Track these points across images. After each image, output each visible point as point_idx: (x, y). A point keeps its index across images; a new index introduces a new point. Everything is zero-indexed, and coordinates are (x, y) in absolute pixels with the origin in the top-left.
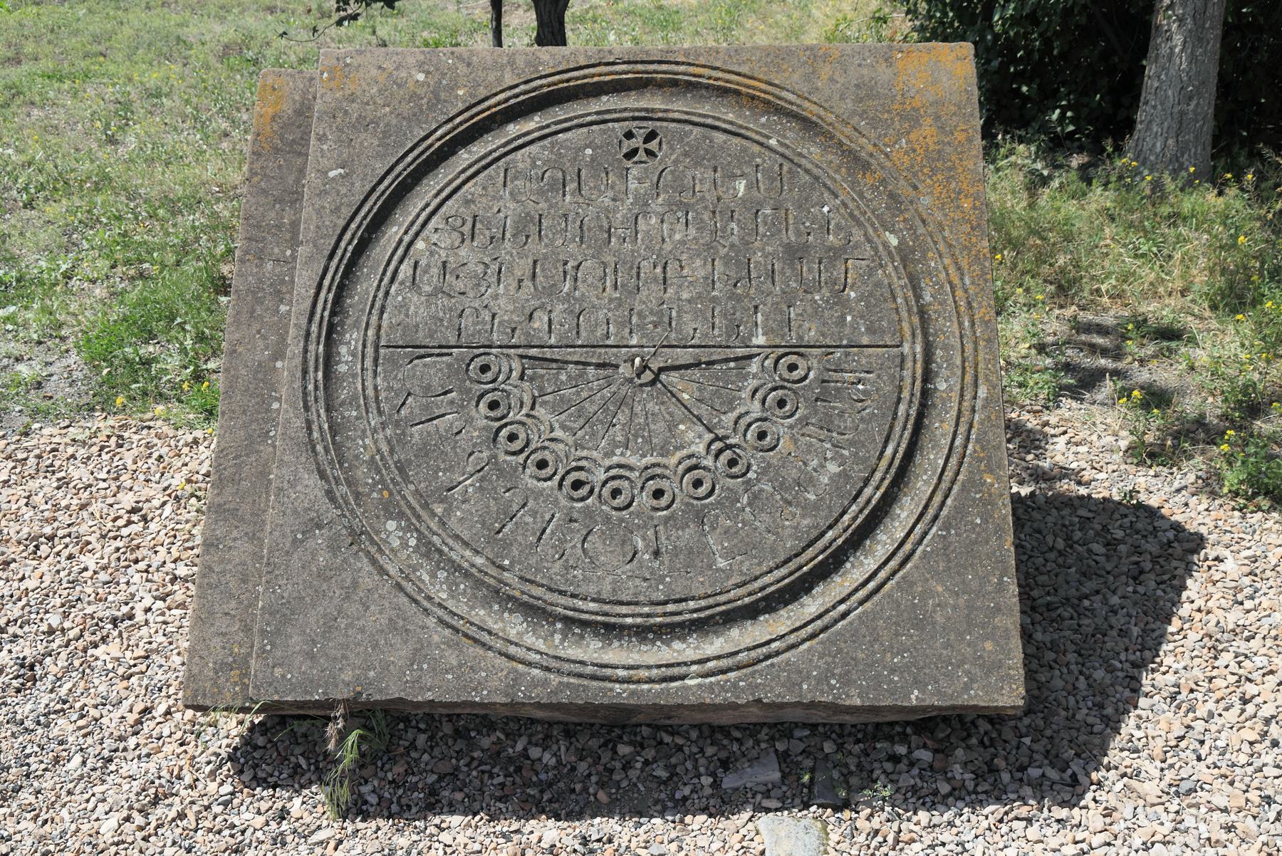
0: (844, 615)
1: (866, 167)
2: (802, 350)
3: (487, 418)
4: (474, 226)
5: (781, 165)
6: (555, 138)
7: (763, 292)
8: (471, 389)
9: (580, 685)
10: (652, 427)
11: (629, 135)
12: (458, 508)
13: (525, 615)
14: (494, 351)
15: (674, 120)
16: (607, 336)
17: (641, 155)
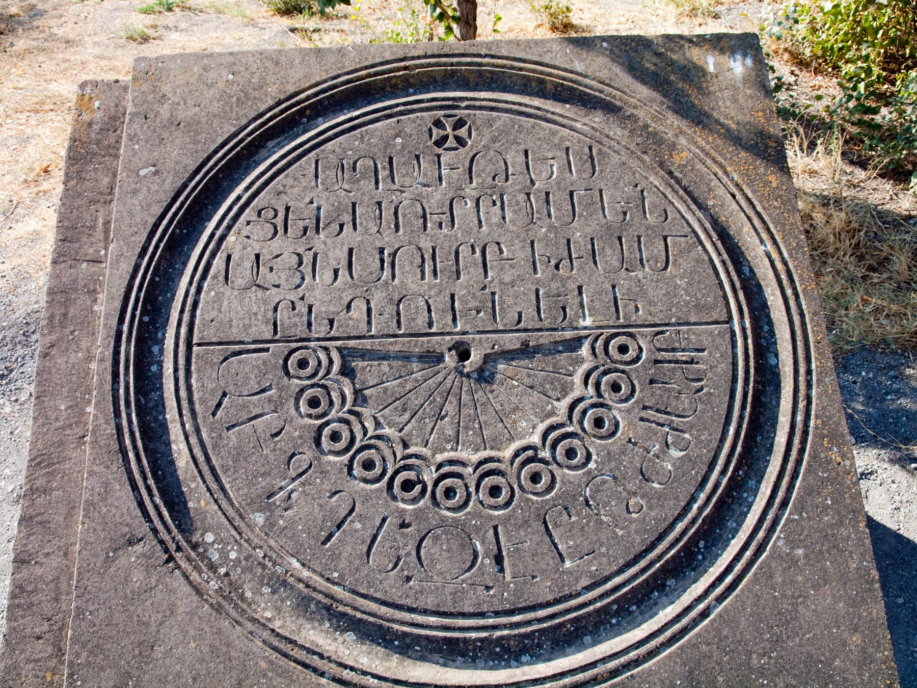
0: (704, 614)
5: (590, 148)
10: (482, 418)
11: (438, 123)
14: (312, 344)
15: (481, 108)
16: (430, 325)
17: (452, 142)
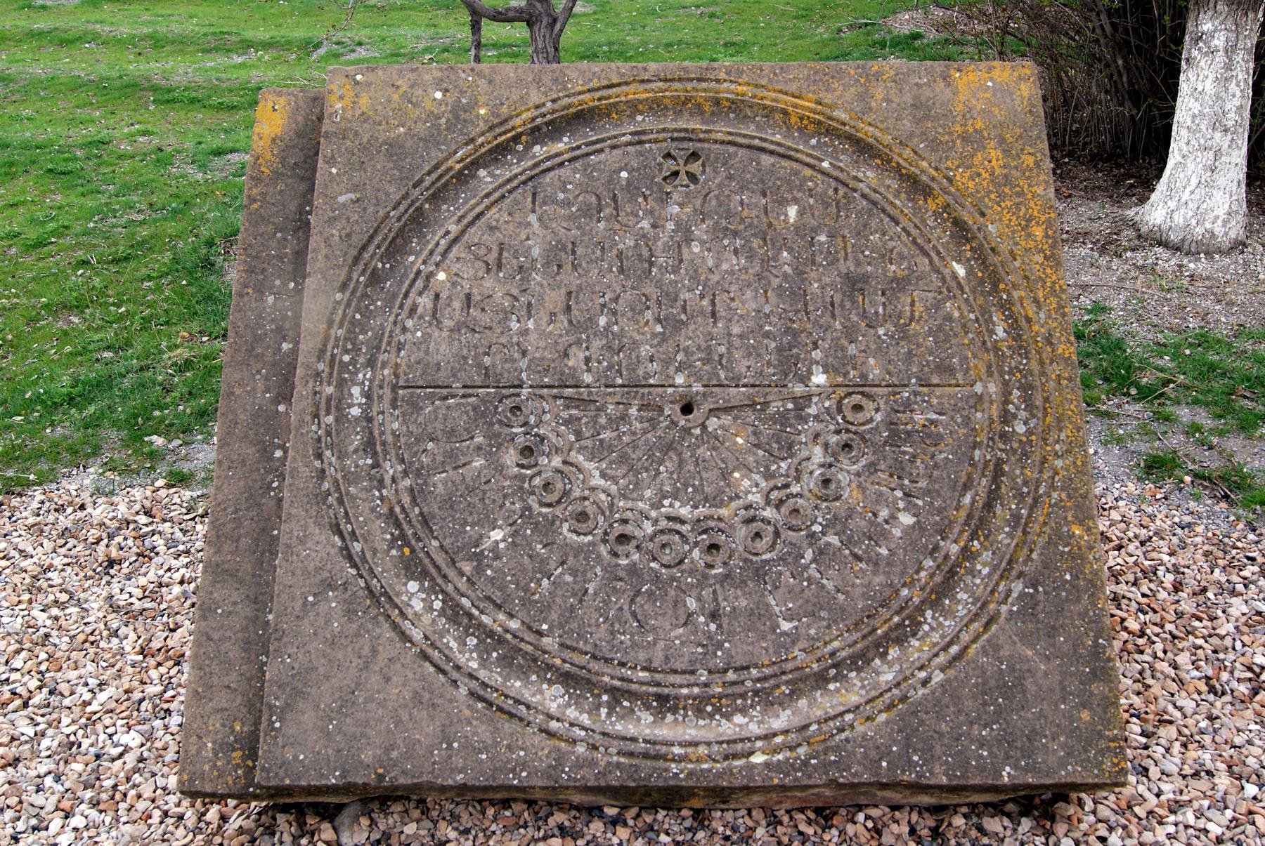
1: (927, 192)
2: (867, 389)
3: (518, 465)
4: (500, 254)
6: (586, 160)
7: (821, 326)
8: (500, 433)
9: (631, 765)
12: (489, 566)
13: (566, 686)
15: (716, 142)
17: (683, 177)
